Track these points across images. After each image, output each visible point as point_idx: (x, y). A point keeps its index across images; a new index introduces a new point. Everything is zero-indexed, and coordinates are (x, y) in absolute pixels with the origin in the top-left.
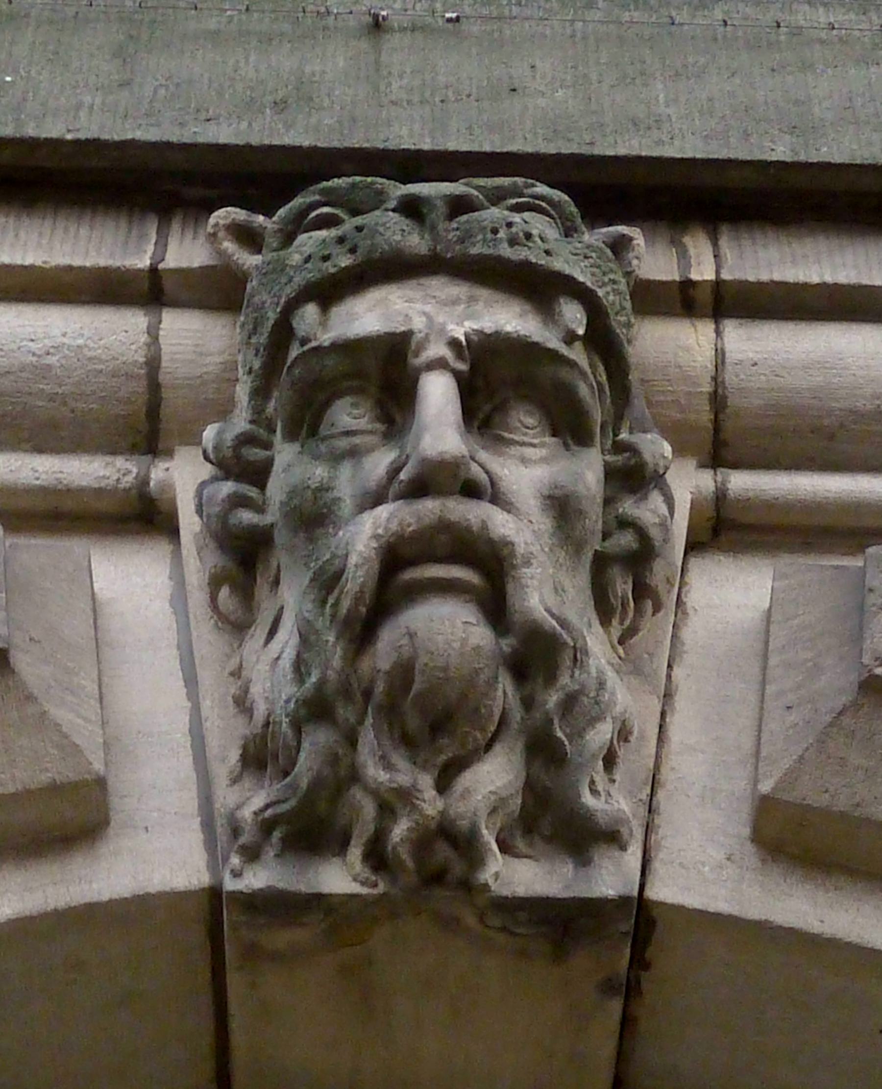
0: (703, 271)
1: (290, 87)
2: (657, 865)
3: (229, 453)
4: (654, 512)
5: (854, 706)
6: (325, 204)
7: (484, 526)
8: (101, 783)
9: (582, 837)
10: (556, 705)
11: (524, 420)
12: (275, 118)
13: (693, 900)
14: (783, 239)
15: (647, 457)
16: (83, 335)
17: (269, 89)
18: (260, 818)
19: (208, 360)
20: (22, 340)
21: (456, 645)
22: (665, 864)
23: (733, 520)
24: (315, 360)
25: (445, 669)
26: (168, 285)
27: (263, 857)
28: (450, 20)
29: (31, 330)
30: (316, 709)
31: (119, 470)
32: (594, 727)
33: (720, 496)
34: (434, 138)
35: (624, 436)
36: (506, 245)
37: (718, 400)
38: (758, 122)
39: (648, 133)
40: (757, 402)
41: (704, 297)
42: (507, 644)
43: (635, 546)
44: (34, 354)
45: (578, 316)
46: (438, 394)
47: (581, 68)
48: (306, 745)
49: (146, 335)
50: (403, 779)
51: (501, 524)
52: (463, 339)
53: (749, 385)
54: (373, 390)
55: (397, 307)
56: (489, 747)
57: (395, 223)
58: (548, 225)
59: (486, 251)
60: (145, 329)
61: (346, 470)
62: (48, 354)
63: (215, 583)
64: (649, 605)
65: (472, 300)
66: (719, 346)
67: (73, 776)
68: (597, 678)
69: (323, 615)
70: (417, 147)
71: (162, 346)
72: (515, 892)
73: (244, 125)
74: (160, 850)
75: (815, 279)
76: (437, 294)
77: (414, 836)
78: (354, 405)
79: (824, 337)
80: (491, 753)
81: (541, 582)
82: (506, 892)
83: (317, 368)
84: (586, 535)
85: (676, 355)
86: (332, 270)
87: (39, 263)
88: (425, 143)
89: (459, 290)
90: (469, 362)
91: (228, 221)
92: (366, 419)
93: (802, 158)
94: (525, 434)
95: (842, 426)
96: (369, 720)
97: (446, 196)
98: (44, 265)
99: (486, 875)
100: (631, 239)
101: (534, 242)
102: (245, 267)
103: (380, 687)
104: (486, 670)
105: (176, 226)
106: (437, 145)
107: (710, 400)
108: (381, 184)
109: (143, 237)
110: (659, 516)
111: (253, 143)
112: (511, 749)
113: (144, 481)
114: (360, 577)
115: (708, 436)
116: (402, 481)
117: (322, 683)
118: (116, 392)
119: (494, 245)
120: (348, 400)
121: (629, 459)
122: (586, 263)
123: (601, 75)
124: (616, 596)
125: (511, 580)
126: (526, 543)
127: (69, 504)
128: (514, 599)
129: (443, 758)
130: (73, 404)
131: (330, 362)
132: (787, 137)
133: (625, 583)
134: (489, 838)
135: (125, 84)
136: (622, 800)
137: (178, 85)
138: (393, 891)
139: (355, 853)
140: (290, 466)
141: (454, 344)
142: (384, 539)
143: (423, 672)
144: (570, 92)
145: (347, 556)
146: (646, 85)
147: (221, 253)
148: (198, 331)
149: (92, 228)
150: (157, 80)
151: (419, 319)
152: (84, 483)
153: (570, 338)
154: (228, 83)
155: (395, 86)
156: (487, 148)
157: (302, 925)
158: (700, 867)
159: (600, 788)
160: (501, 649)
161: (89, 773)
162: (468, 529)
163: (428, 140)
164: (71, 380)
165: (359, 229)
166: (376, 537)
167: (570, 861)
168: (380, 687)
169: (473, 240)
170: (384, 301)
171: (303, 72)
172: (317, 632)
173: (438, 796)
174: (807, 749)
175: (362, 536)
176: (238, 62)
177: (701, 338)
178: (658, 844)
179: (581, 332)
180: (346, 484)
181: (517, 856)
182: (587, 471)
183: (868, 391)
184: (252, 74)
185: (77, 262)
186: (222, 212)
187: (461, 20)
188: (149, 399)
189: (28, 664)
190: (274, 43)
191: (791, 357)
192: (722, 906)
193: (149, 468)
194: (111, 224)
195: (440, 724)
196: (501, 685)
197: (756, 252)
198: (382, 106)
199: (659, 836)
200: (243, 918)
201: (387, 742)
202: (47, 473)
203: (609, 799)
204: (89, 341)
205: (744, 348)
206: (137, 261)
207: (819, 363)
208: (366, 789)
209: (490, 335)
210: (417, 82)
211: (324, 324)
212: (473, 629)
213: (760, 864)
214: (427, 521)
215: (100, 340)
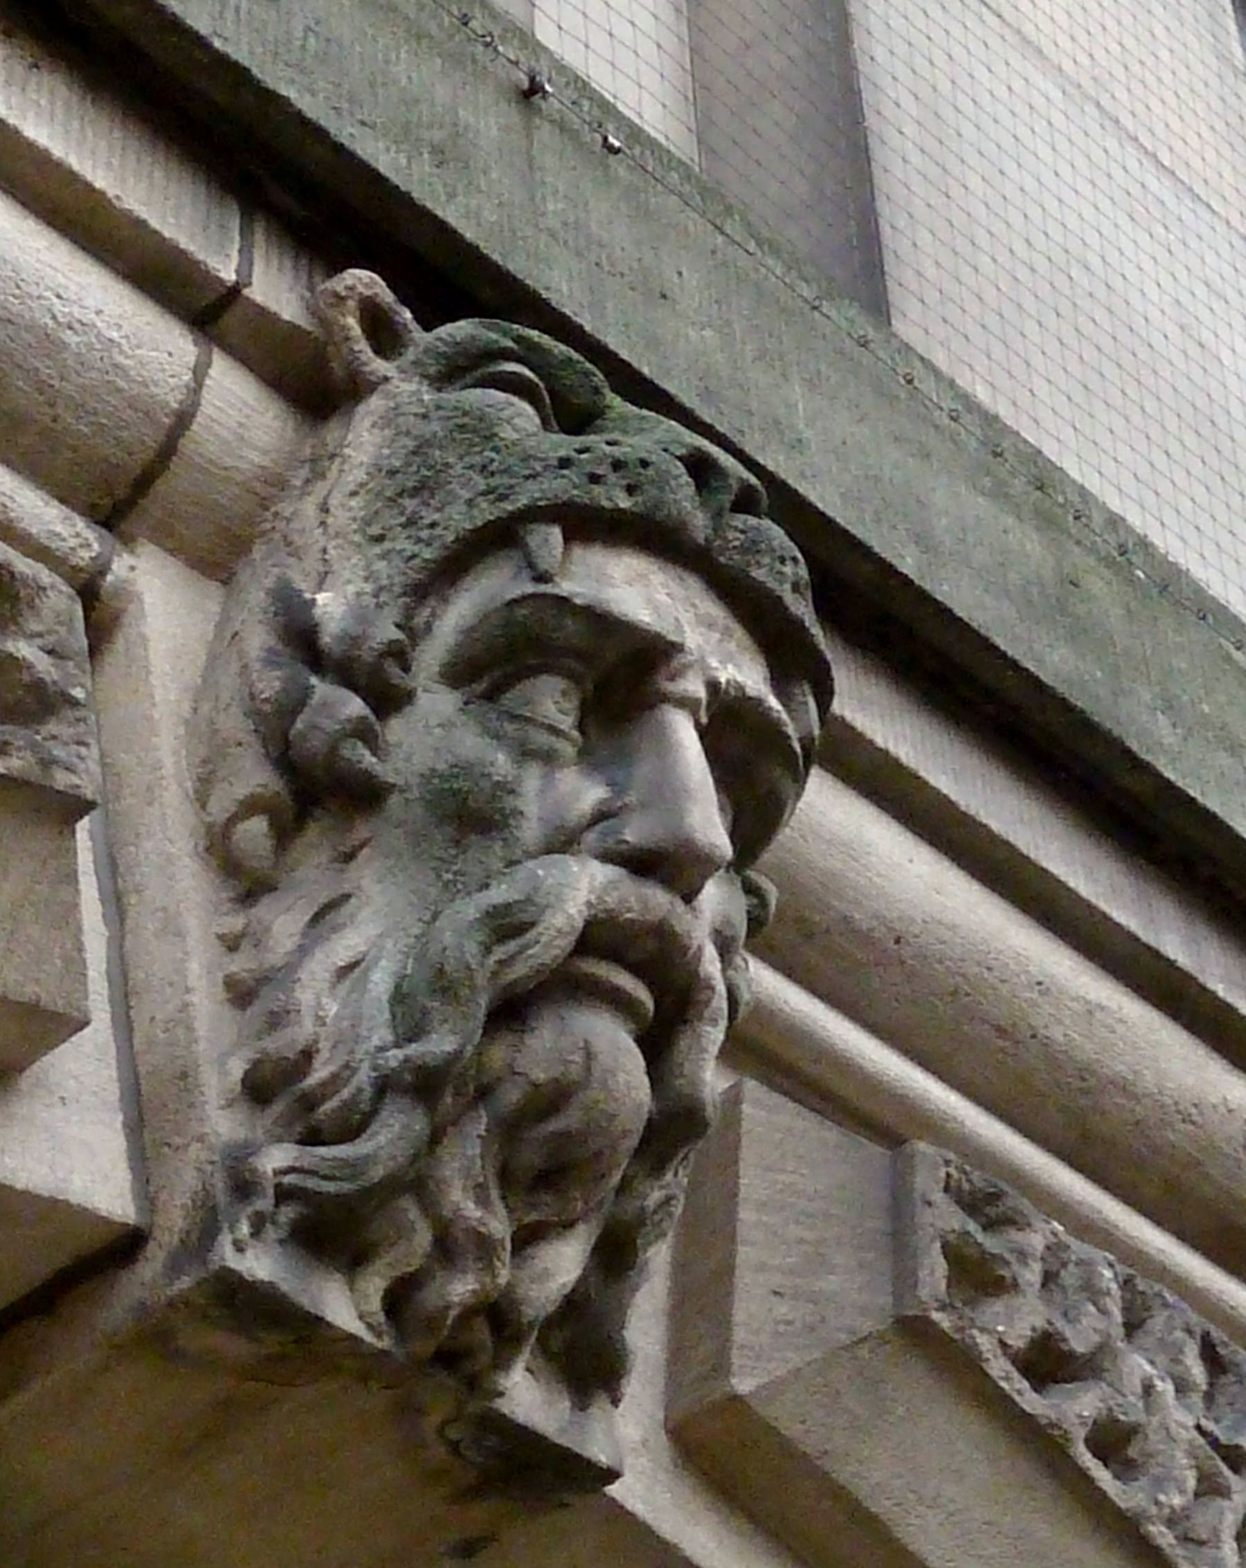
6: (519, 360)
16: (120, 327)
20: (48, 288)
25: (612, 1117)
29: (63, 280)
31: (78, 535)
49: (190, 375)
60: (192, 365)
62: (70, 328)
71: (203, 402)
75: (880, 742)
95: (827, 931)
98: (115, 201)
102: (367, 369)
103: (511, 1096)
114: (558, 947)
139: (375, 1285)
169: (758, 557)
172: (473, 988)
174: (809, 1364)
186: (365, 274)
204: (123, 341)
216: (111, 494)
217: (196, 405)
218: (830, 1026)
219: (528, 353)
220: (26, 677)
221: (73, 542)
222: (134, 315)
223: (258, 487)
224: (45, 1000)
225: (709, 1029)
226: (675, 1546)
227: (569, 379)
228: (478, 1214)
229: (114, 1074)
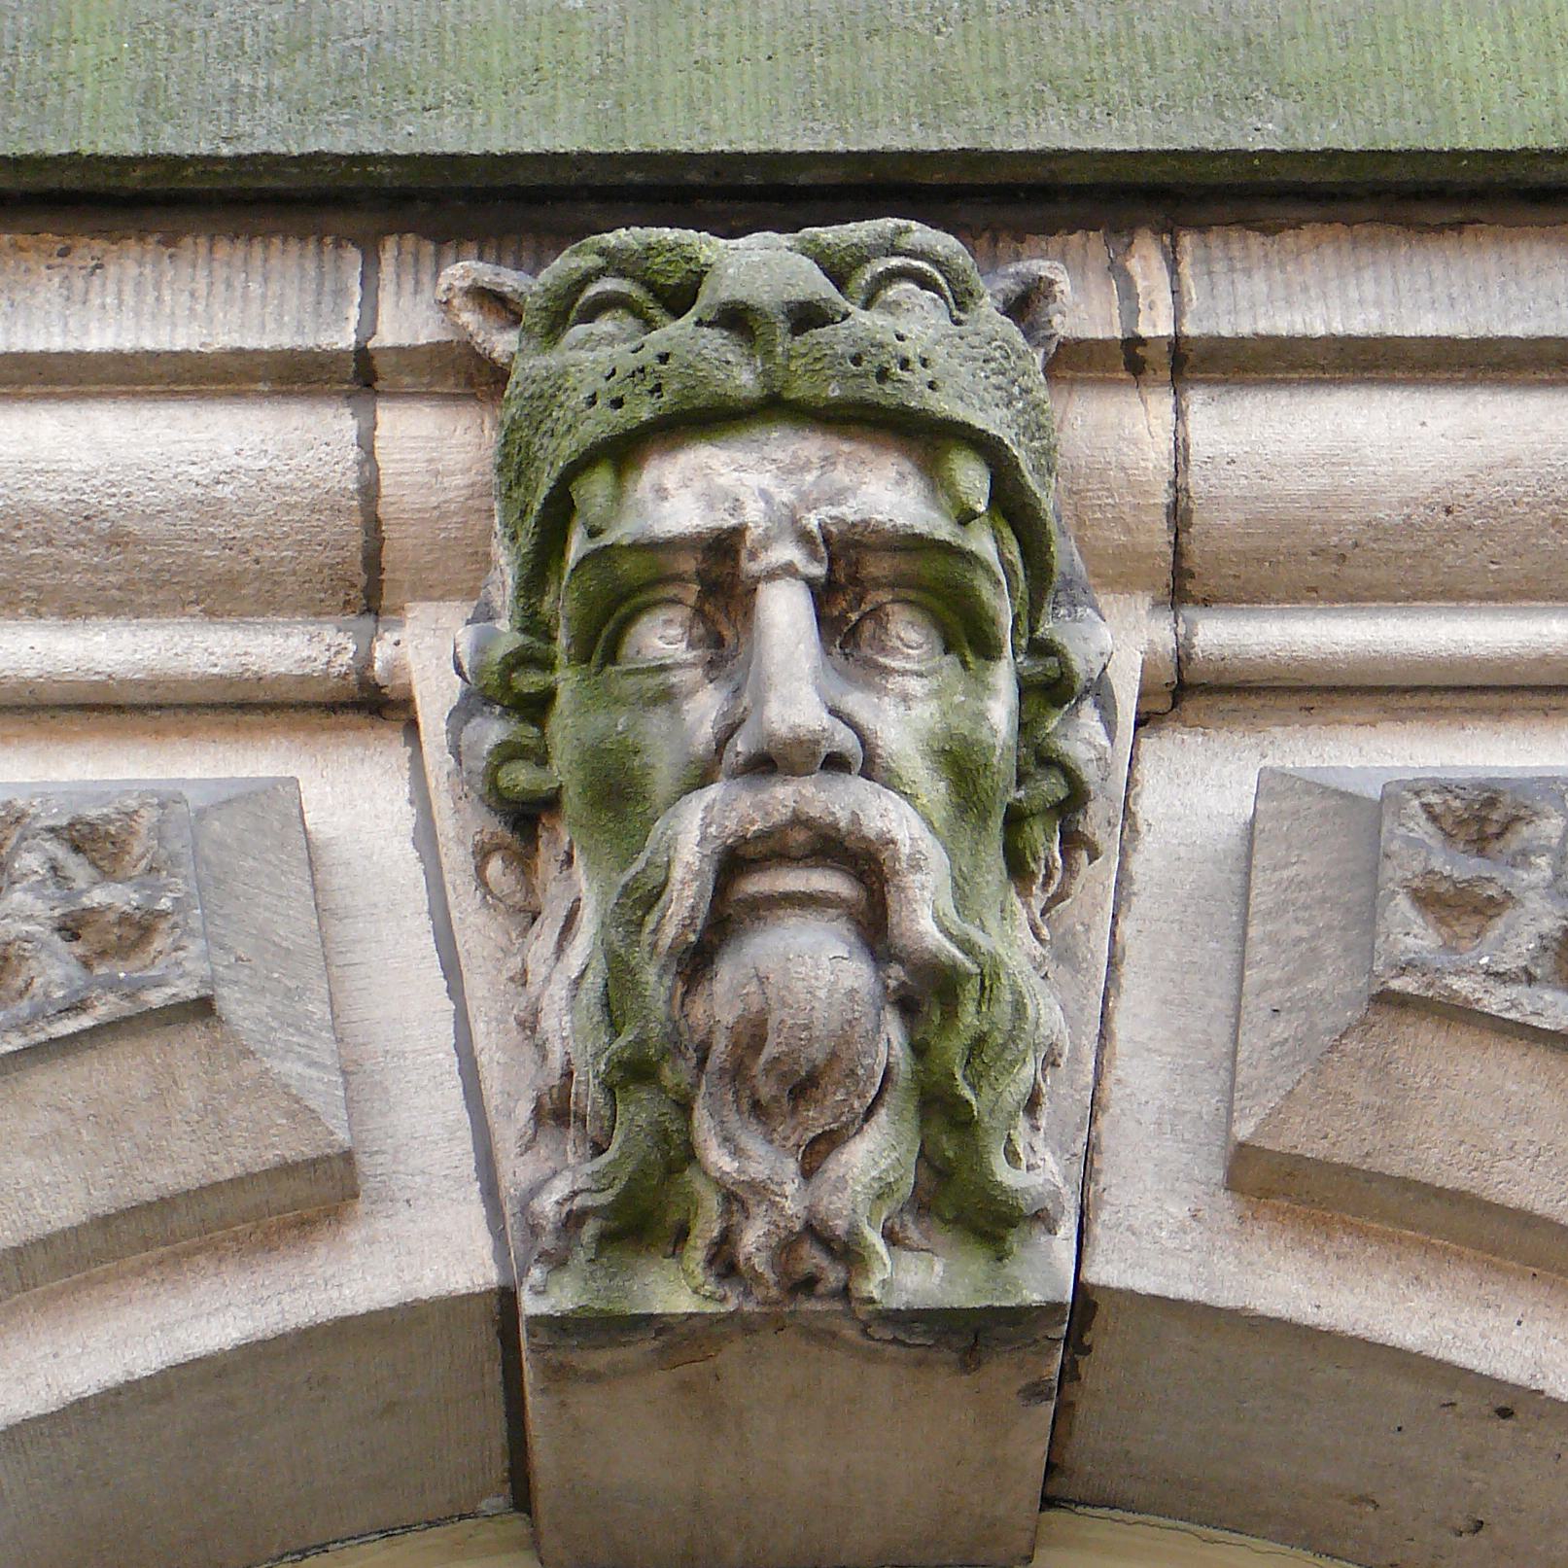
0: (1157, 325)
3: (495, 680)
7: (855, 818)
8: (348, 1157)
13: (1146, 1283)
19: (447, 482)
21: (822, 994)
25: (807, 1028)
26: (380, 364)
33: (1183, 657)
37: (1178, 515)
41: (1161, 358)
46: (785, 615)
50: (758, 1170)
55: (721, 481)
56: (870, 1112)
63: (482, 854)
67: (310, 1153)
75: (1320, 330)
76: (779, 455)
78: (668, 622)
87: (195, 347)
91: (466, 283)
99: (872, 1288)
103: (721, 1045)
106: (766, 142)
107: (1168, 515)
115: (1165, 564)
116: (738, 754)
117: (640, 1043)
130: (256, 552)
134: (874, 1238)
136: (1048, 1156)
138: (749, 1307)
139: (696, 1254)
145: (669, 863)
153: (965, 517)
161: (331, 1147)
164: (254, 520)
165: (664, 358)
168: (721, 1045)
175: (690, 833)
177: (1153, 422)
178: (1099, 1197)
179: (981, 508)
183: (1394, 496)
185: (250, 343)
189: (238, 1002)
192: (1187, 1291)
195: (803, 1088)
199: (1101, 1186)
201: (733, 1120)
206: (336, 338)
209: (854, 525)
211: (618, 497)
214: (776, 818)
218: (1406, 636)
219: (615, 263)
220: (112, 917)
222: (278, 431)
223: (476, 503)
224: (291, 1155)
226: (1244, 1308)
229: (470, 1146)
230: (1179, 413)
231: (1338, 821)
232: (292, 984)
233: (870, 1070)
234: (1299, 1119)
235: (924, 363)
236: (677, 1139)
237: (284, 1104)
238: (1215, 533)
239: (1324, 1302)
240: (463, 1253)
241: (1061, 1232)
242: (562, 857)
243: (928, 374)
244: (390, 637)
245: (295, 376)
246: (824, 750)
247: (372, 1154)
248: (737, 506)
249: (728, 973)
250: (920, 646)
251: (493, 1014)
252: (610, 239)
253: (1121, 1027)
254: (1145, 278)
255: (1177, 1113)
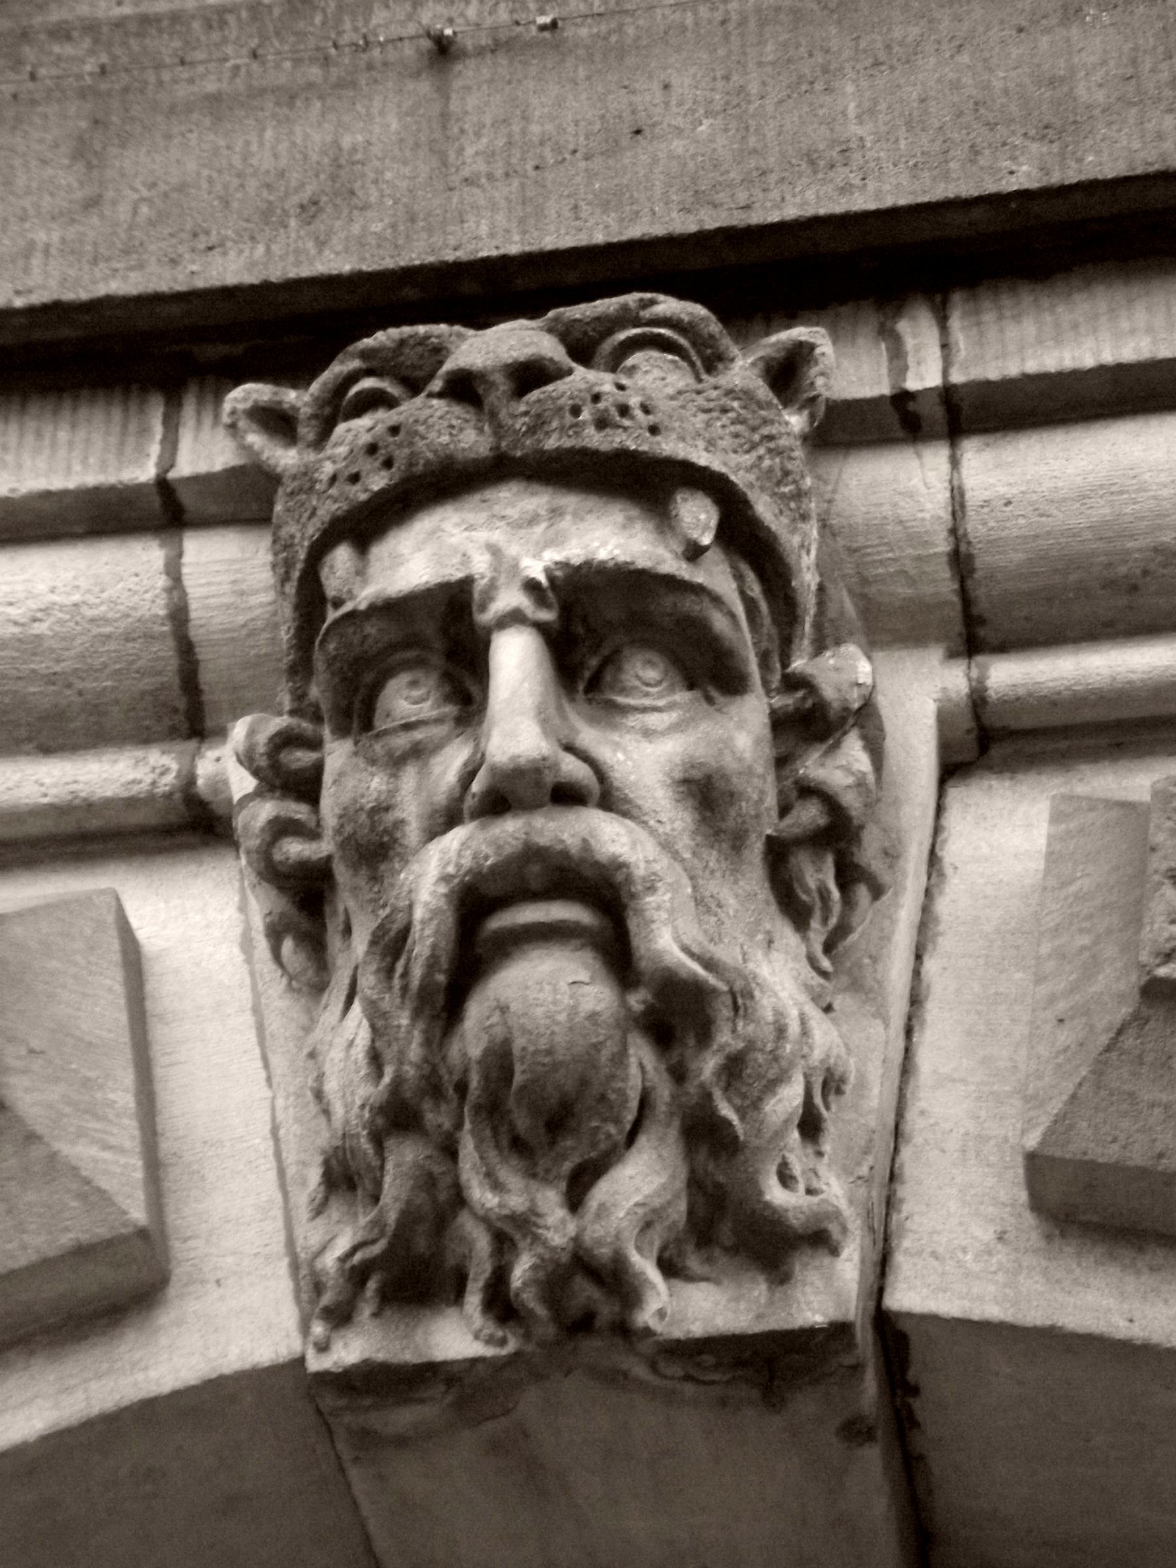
0: (925, 376)
1: (322, 176)
2: (901, 1260)
4: (848, 770)
5: (1137, 1020)
6: (369, 373)
9: (775, 1247)
10: (714, 1074)
11: (644, 674)
12: (302, 233)
13: (949, 1306)
14: (1045, 302)
15: (829, 692)
17: (294, 184)
18: (348, 1265)
19: (254, 600)
21: (562, 1017)
22: (911, 1255)
23: (1004, 728)
24: (351, 630)
25: (549, 1052)
26: (186, 498)
27: (357, 1319)
28: (543, 28)
30: (396, 1117)
31: (154, 769)
32: (775, 1094)
33: (978, 700)
34: (524, 232)
35: (798, 664)
36: (591, 430)
37: (961, 561)
38: (992, 126)
39: (832, 174)
40: (1019, 557)
41: (934, 412)
42: (637, 1000)
43: (822, 821)
44: (16, 623)
45: (703, 517)
47: (735, 77)
48: (389, 1166)
50: (517, 1202)
51: (610, 837)
52: (542, 579)
53: (1003, 534)
54: (436, 659)
55: (453, 540)
56: (631, 1139)
57: (441, 418)
58: (671, 366)
59: (567, 443)
61: (409, 777)
64: (862, 893)
65: (556, 513)
66: (956, 483)
67: (102, 1232)
68: (776, 1022)
69: (390, 988)
70: (502, 251)
71: (189, 590)
72: (689, 1332)
73: (260, 249)
74: (242, 1309)
75: (1089, 362)
76: (509, 512)
77: (541, 1275)
78: (414, 684)
79: (1108, 447)
80: (634, 1149)
81: (671, 911)
82: (678, 1333)
83: (356, 639)
84: (744, 822)
85: (895, 505)
86: (363, 497)
88: (512, 243)
89: (537, 500)
90: (556, 605)
91: (248, 405)
92: (429, 703)
93: (1056, 178)
94: (647, 695)
95: (1145, 573)
96: (467, 1126)
97: (507, 366)
99: (646, 1317)
100: (812, 347)
101: (632, 418)
103: (475, 1081)
104: (609, 1043)
105: (189, 410)
108: (438, 337)
109: (144, 431)
110: (853, 774)
111: (273, 279)
112: (661, 1139)
113: (189, 780)
115: (954, 612)
116: (474, 795)
118: (133, 662)
119: (576, 433)
120: (404, 678)
121: (804, 699)
122: (725, 419)
123: (764, 84)
124: (807, 891)
125: (631, 913)
126: (647, 862)
127: (94, 824)
128: (639, 943)
129: (567, 1166)
130: (79, 685)
131: (371, 629)
132: (1034, 147)
133: (819, 870)
135: (92, 203)
136: (833, 1181)
137: (166, 195)
138: (529, 1348)
139: (473, 1300)
140: (347, 774)
141: (532, 586)
142: (456, 881)
143: (522, 1059)
144: (719, 121)
145: (411, 907)
146: (828, 90)
147: (246, 449)
148: (232, 561)
149: (74, 426)
150: (136, 190)
151: (481, 558)
152: (109, 794)
153: (694, 553)
154: (236, 182)
155: (470, 151)
156: (599, 238)
157: (422, 1401)
158: (960, 1255)
159: (797, 1169)
160: (629, 1009)
162: (565, 854)
163: (516, 238)
166: (445, 878)
167: (761, 1278)
168: (475, 1081)
169: (546, 428)
170: (433, 533)
171: (340, 149)
173: (568, 1217)
174: (1080, 1084)
175: (429, 875)
176: (248, 143)
178: (901, 1226)
179: (706, 540)
180: (412, 796)
181: (690, 1278)
182: (741, 732)
184: (268, 163)
185: (57, 483)
187: (560, 24)
188: (181, 666)
190: (299, 103)
191: (1060, 484)
192: (993, 1312)
193: (193, 760)
194: (98, 415)
195: (559, 1119)
196: (633, 1061)
197: (1001, 331)
198: (451, 189)
199: (904, 1215)
200: (342, 1402)
201: (492, 1154)
202: (55, 785)
203: (812, 1185)
205: (991, 481)
207: (1101, 486)
208: (475, 1215)
209: (580, 567)
210: (501, 142)
211: (361, 573)
212: (587, 989)
213: (1042, 1244)
214: (508, 850)
215: (102, 591)
216: (176, 711)
217: (184, 594)
219: (375, 365)
221: (148, 779)
224: (85, 1238)
225: (648, 899)
227: (410, 356)
228: (496, 1200)
230: (955, 462)
231: (1117, 830)
232: (92, 1074)
233: (622, 1093)
234: (1085, 1124)
235: (646, 410)
236: (448, 1180)
237: (74, 1186)
238: (999, 576)
239: (1137, 1315)
240: (269, 1327)
241: (845, 1254)
242: (341, 928)
243: (651, 419)
244: (211, 754)
245: (101, 516)
246: (549, 779)
247: (185, 1240)
248: (466, 558)
249: (476, 1010)
250: (659, 683)
251: (292, 1089)
252: (367, 342)
253: (926, 1060)
254: (915, 336)
255: (982, 1139)
